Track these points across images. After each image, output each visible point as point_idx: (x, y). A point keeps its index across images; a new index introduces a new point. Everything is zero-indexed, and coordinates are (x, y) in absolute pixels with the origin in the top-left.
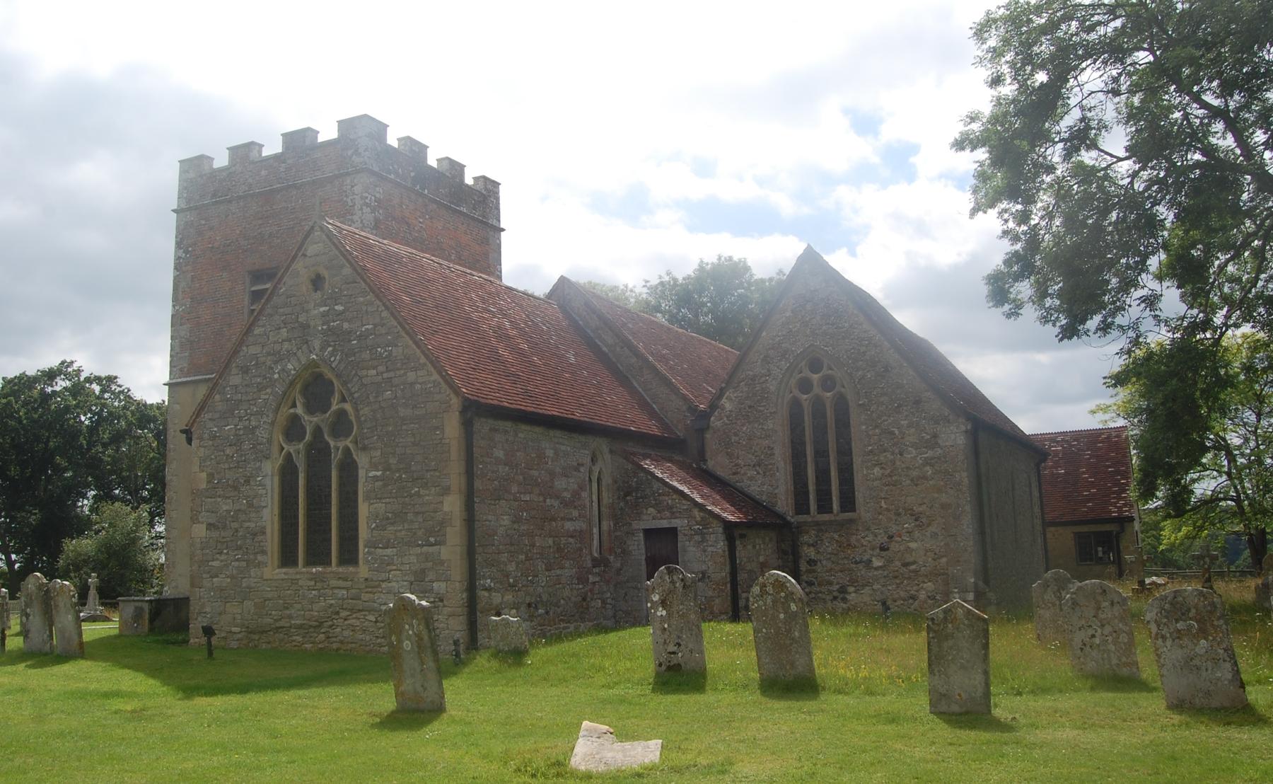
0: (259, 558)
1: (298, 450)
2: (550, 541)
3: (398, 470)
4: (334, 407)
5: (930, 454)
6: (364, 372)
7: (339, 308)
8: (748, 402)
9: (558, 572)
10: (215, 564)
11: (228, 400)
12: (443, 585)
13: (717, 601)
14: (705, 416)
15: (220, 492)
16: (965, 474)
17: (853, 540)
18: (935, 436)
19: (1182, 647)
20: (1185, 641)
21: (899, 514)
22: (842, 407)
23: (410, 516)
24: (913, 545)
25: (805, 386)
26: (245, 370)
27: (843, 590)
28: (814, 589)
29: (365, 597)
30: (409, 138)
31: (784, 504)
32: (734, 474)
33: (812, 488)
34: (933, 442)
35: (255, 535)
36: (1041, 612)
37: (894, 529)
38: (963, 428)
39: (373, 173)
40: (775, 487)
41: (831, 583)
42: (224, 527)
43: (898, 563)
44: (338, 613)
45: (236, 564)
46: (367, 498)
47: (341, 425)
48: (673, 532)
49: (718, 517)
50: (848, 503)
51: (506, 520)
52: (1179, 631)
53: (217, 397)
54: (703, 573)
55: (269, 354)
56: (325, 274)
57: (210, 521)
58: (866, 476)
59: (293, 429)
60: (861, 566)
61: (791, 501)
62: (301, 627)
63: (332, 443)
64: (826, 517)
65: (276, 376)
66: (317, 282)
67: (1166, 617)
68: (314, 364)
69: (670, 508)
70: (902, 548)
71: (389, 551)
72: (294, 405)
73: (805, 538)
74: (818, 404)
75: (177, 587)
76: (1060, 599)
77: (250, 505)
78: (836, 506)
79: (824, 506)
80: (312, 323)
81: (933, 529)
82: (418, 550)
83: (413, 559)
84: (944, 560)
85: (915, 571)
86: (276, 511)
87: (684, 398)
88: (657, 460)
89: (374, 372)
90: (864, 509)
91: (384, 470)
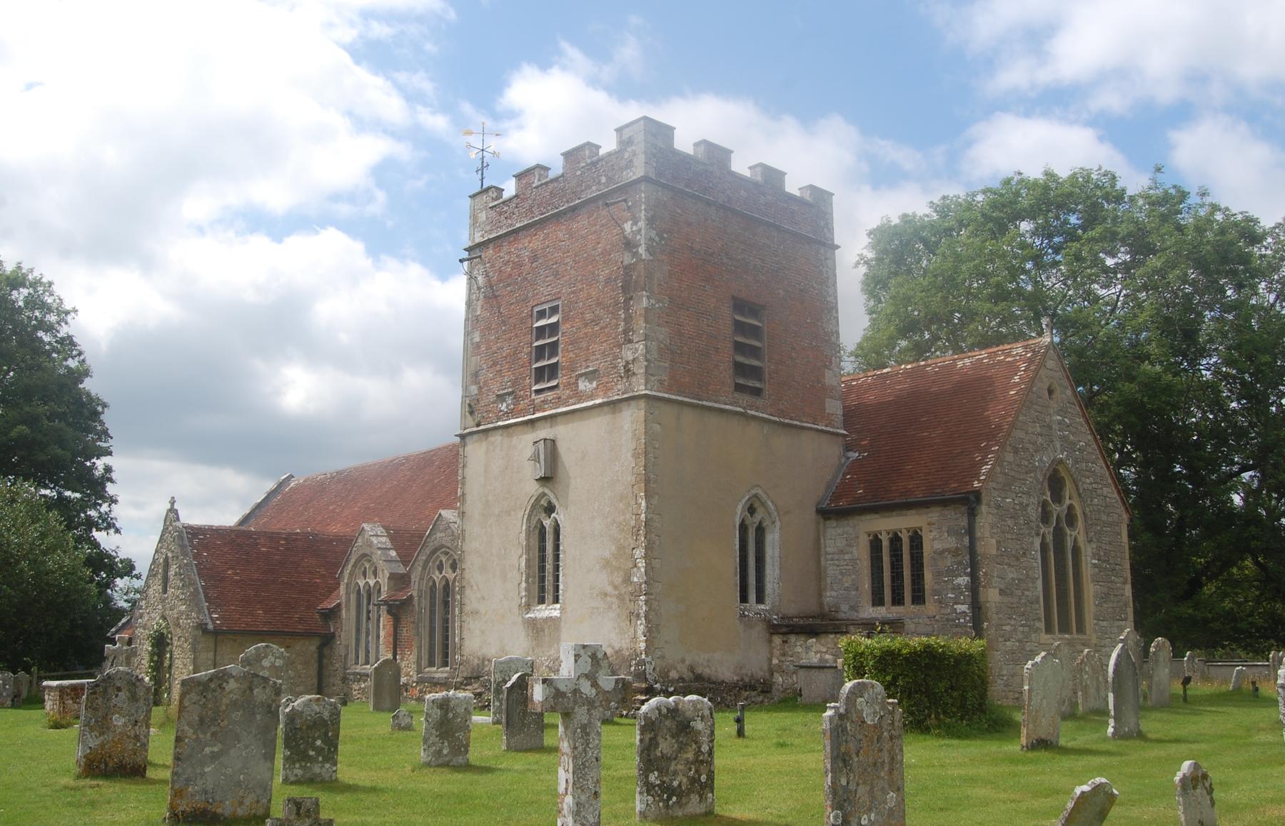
0: (1037, 624)
1: (1048, 531)
4: (1068, 502)
10: (1008, 628)
26: (1016, 451)
42: (1012, 594)
46: (1096, 581)
47: (1071, 519)
57: (1002, 587)
66: (1050, 392)
71: (1105, 623)
75: (662, 657)
77: (1027, 575)
82: (1117, 623)
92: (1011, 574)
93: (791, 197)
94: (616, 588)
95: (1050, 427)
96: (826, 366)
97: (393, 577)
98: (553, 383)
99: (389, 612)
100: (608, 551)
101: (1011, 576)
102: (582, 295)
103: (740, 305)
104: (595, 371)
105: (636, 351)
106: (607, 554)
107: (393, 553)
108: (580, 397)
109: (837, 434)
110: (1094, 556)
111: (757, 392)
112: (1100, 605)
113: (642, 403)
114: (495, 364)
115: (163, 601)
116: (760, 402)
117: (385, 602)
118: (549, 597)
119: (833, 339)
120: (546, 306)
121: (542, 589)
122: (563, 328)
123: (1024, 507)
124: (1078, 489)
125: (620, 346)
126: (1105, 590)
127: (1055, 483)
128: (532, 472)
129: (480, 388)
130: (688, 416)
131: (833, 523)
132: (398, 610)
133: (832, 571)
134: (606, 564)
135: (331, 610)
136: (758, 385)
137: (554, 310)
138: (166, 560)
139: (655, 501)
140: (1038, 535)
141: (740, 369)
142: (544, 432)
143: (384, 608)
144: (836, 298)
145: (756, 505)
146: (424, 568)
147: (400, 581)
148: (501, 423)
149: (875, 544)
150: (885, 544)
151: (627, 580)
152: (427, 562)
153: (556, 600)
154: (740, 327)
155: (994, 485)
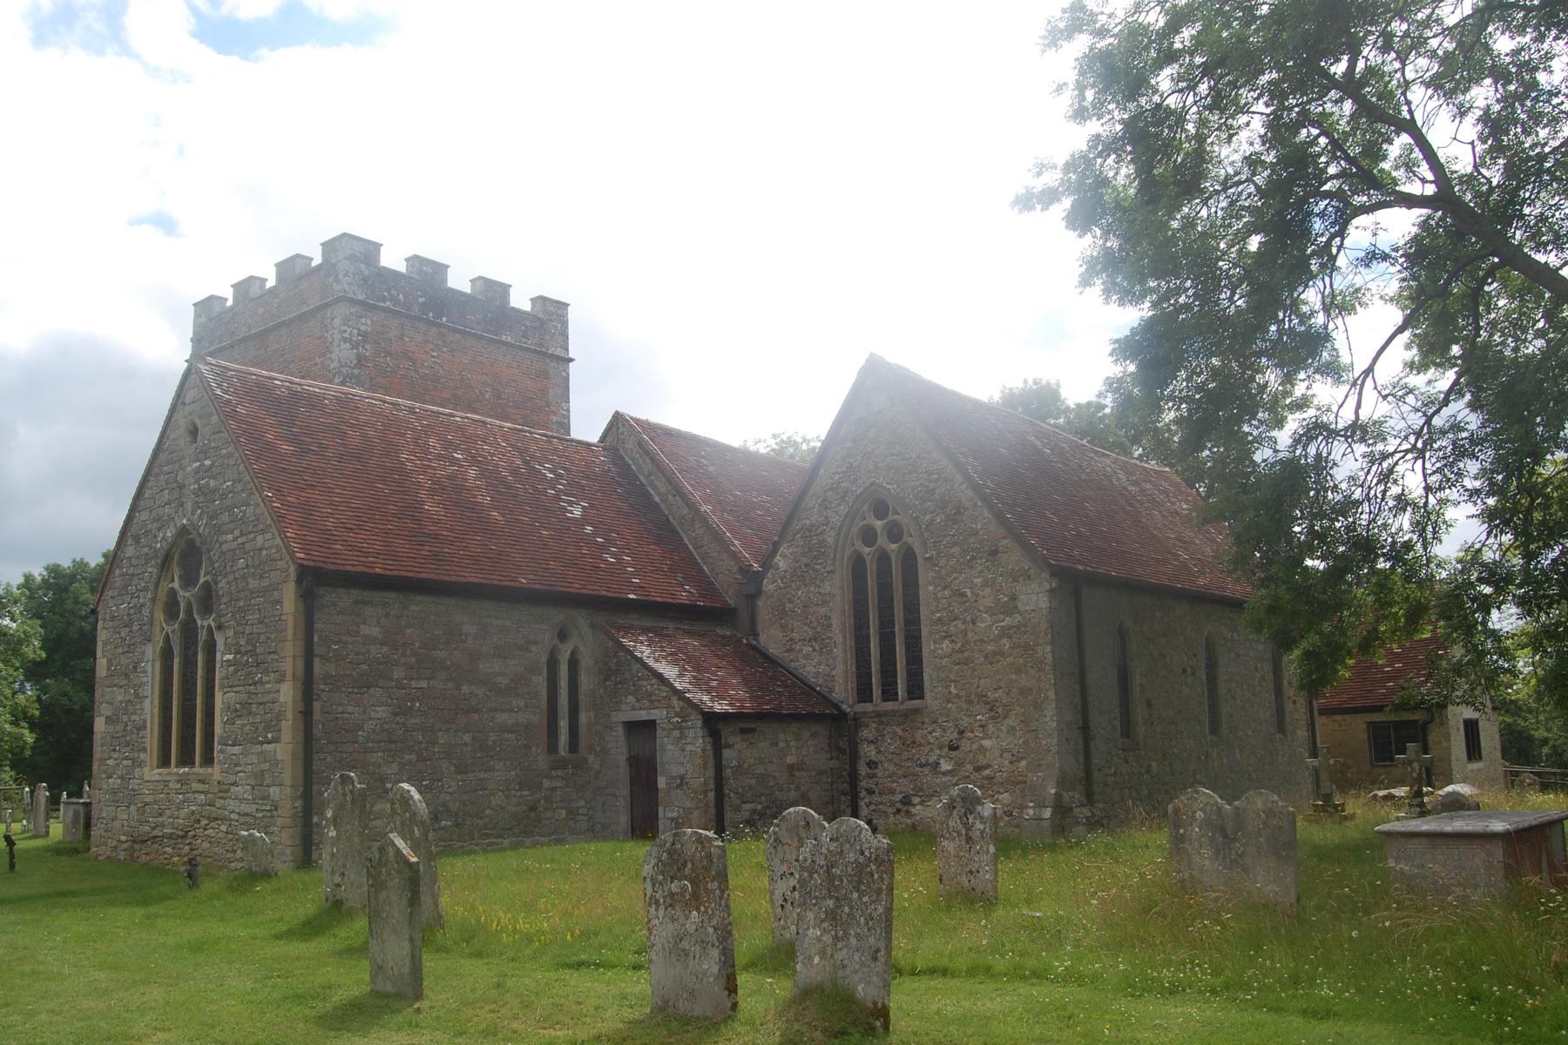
2: (467, 738)
4: (202, 580)
5: (1008, 621)
8: (805, 560)
9: (482, 775)
10: (110, 762)
12: (277, 790)
13: (696, 814)
14: (757, 578)
16: (1048, 648)
17: (918, 734)
18: (1014, 598)
19: (673, 920)
20: (678, 912)
21: (970, 702)
22: (909, 558)
24: (987, 743)
25: (869, 536)
27: (906, 801)
28: (876, 798)
29: (219, 803)
30: (416, 257)
31: (842, 691)
32: (790, 650)
33: (875, 667)
34: (1010, 607)
36: (945, 843)
37: (965, 721)
38: (1047, 586)
39: (354, 302)
40: (829, 668)
41: (892, 792)
43: (969, 767)
44: (198, 821)
48: (650, 725)
49: (695, 707)
50: (916, 690)
51: (381, 712)
52: (672, 894)
54: (682, 777)
55: (155, 520)
56: (198, 423)
58: (935, 650)
60: (926, 770)
61: (852, 685)
62: (170, 836)
64: (889, 706)
67: (662, 873)
68: (183, 531)
69: (649, 695)
70: (975, 746)
71: (236, 750)
73: (865, 733)
74: (883, 558)
76: (968, 827)
77: (137, 695)
78: (877, 692)
79: (889, 694)
81: (1010, 722)
82: (258, 748)
84: (1023, 763)
85: (989, 778)
86: (156, 702)
87: (735, 556)
88: (658, 636)
89: (230, 537)
90: (931, 700)
91: (237, 653)
101: (120, 698)
112: (231, 722)
126: (244, 696)
155: (110, 593)
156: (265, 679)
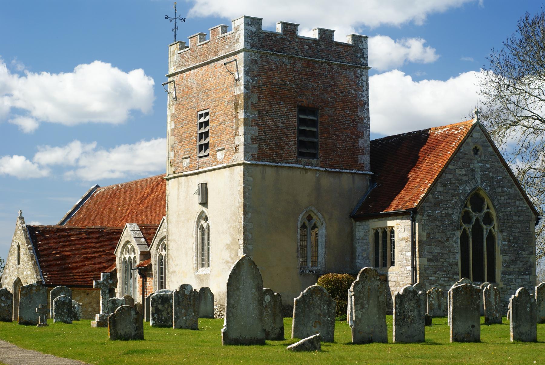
0: (455, 277)
1: (469, 228)
3: (513, 243)
4: (485, 210)
6: (499, 198)
7: (488, 166)
11: (436, 198)
15: (434, 243)
23: (518, 262)
26: (445, 185)
35: (452, 265)
42: (437, 260)
45: (443, 279)
46: (503, 252)
47: (488, 219)
53: (430, 196)
55: (456, 180)
57: (430, 257)
59: (466, 218)
63: (484, 227)
65: (461, 191)
66: (476, 150)
71: (511, 277)
72: (466, 206)
77: (450, 251)
80: (476, 170)
82: (521, 277)
83: (520, 280)
89: (503, 198)
92: (437, 251)
93: (339, 44)
94: (232, 259)
95: (473, 170)
96: (359, 137)
97: (142, 254)
98: (206, 154)
99: (140, 273)
100: (228, 240)
101: (436, 251)
102: (219, 108)
103: (302, 110)
104: (224, 149)
105: (240, 140)
106: (229, 243)
107: (143, 240)
108: (218, 162)
109: (365, 174)
110: (505, 240)
111: (314, 156)
113: (242, 167)
114: (181, 142)
115: (18, 269)
116: (314, 161)
117: (138, 268)
118: (206, 263)
119: (365, 121)
120: (203, 112)
121: (203, 260)
122: (210, 124)
123: (449, 215)
124: (493, 203)
125: (234, 137)
127: (477, 201)
128: (197, 199)
129: (175, 154)
130: (269, 171)
131: (358, 223)
132: (145, 272)
133: (359, 250)
134: (228, 247)
135: (111, 273)
136: (314, 151)
137: (207, 114)
138: (19, 246)
139: (249, 215)
140: (458, 229)
141: (301, 144)
142: (202, 179)
143: (137, 271)
144: (368, 97)
145: (312, 215)
146: (157, 249)
147: (146, 256)
148: (184, 173)
149: (376, 234)
150: (380, 234)
151: (236, 255)
152: (158, 245)
153: (209, 266)
154: (301, 122)
156: (523, 253)
